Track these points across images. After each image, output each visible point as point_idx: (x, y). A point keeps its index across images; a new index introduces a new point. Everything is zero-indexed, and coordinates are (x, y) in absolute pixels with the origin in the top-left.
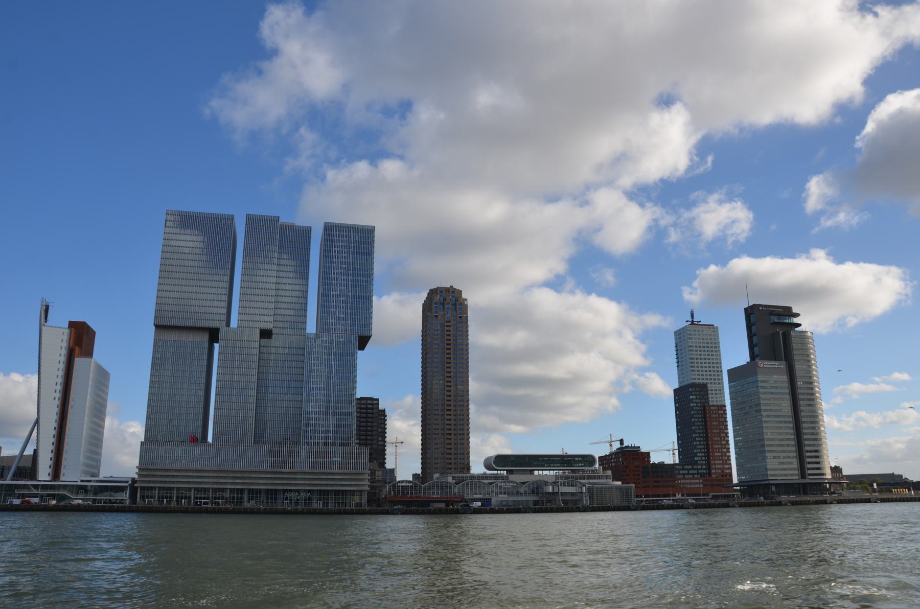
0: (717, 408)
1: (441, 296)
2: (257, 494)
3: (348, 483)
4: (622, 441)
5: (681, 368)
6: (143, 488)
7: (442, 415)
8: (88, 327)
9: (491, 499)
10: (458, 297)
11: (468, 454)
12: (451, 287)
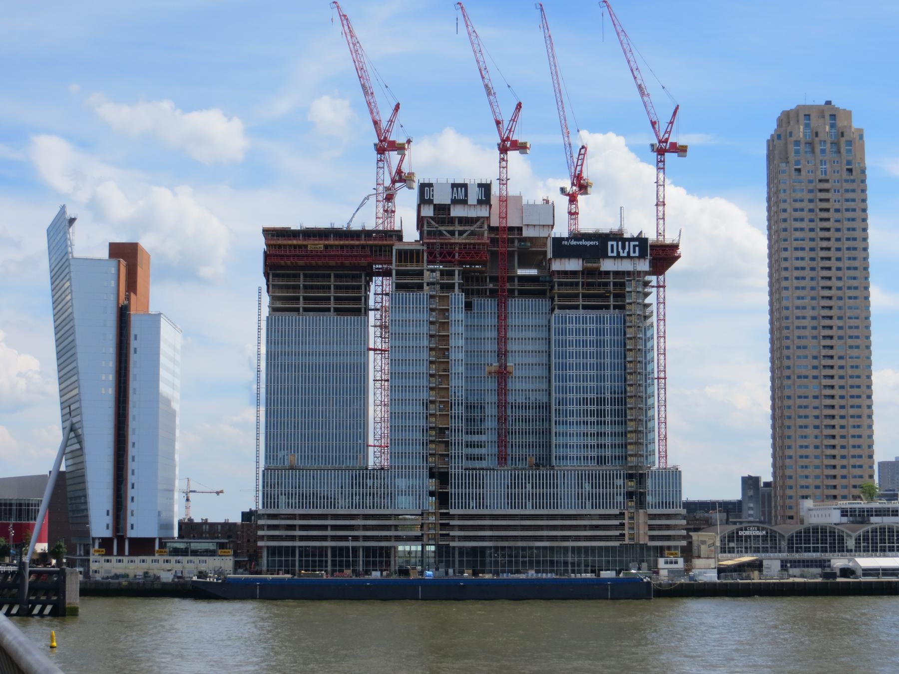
1: (807, 126)
6: (272, 551)
10: (845, 127)
12: (828, 103)
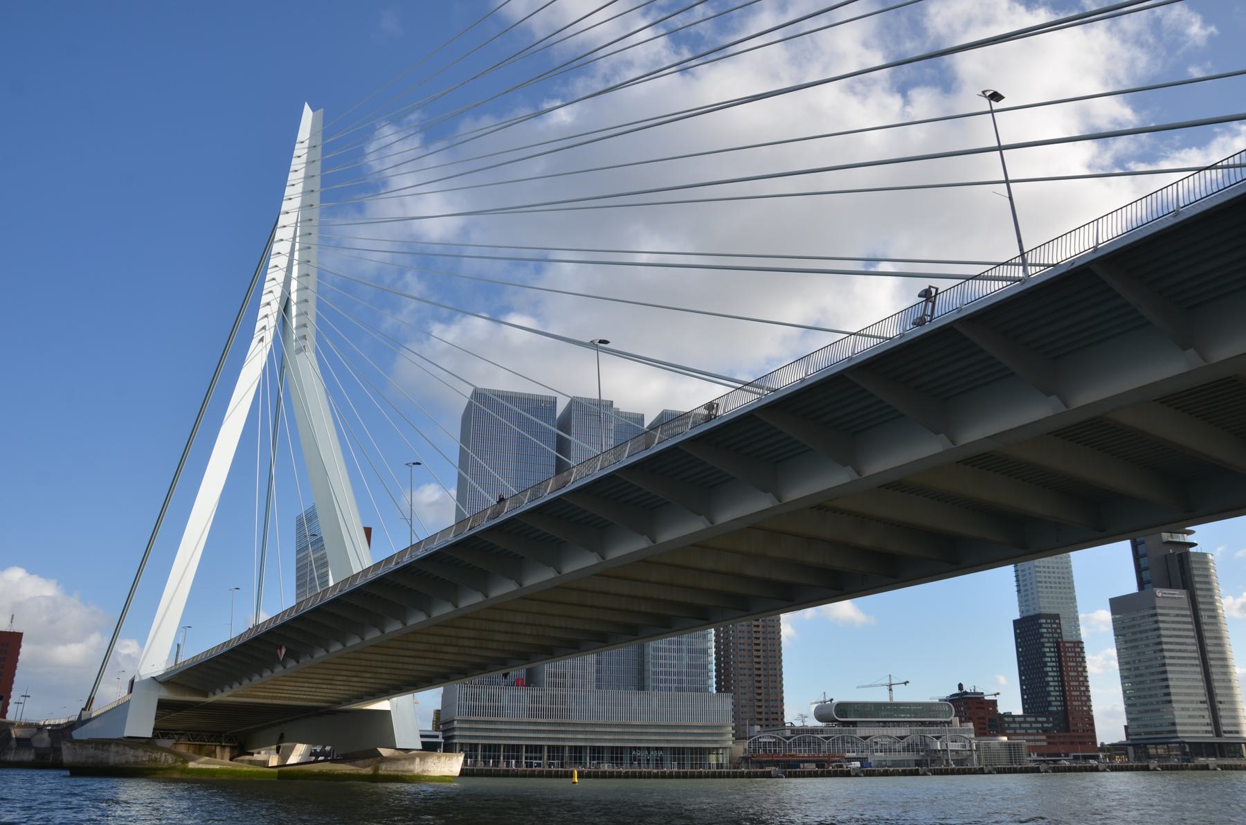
0: (1072, 645)
2: (599, 753)
3: (710, 738)
4: (960, 686)
5: (1023, 593)
7: (749, 650)
9: (867, 758)
11: (782, 700)
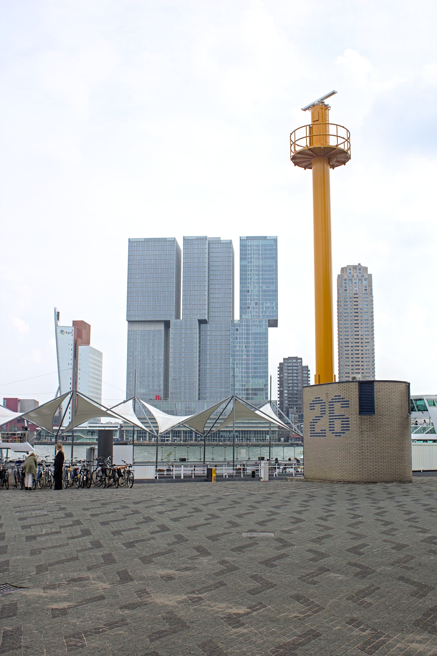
8: (85, 323)
12: (359, 264)
